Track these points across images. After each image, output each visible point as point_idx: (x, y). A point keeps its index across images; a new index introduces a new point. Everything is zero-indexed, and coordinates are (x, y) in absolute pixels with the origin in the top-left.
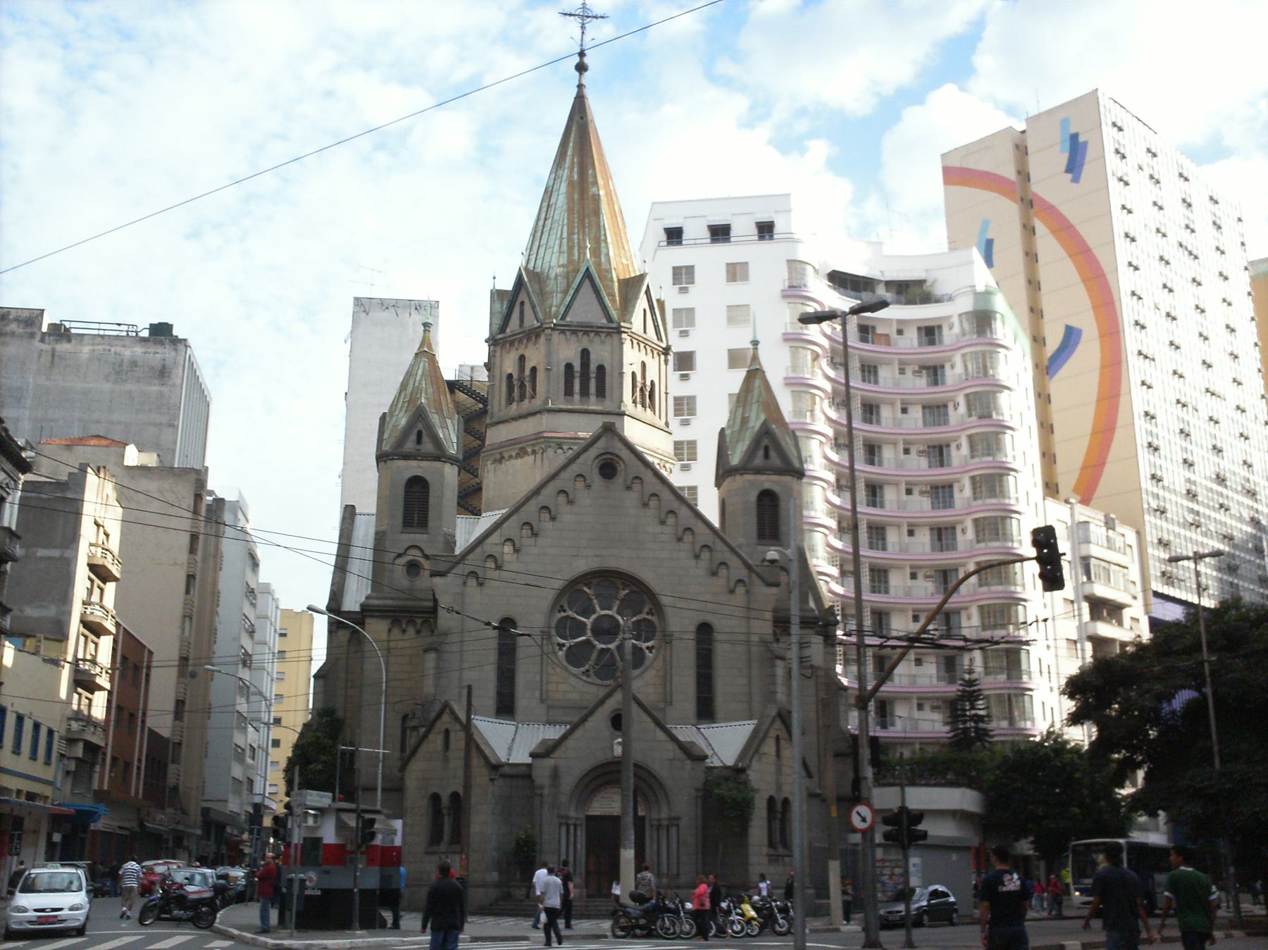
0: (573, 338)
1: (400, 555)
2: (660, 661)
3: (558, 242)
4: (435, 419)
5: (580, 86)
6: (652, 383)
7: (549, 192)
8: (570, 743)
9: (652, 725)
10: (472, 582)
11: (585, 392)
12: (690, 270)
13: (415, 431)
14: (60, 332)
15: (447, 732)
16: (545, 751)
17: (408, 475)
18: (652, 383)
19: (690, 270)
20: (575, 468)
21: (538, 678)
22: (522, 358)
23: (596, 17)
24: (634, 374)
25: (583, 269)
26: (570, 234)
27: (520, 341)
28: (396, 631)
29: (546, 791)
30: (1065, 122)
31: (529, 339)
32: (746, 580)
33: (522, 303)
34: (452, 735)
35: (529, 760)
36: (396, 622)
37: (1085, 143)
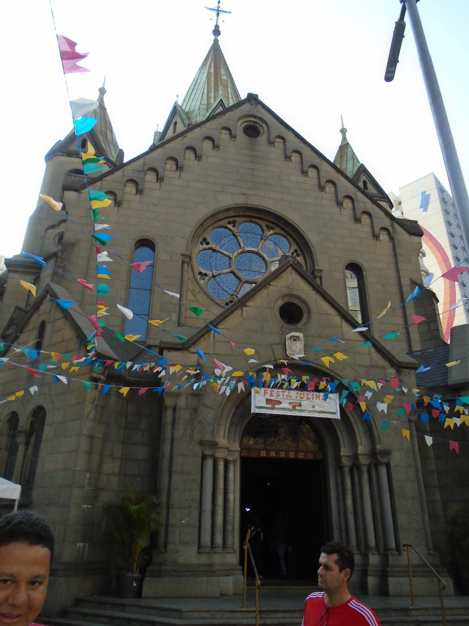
1: (53, 227)
3: (201, 95)
7: (196, 81)
9: (337, 319)
15: (43, 325)
23: (225, 12)
25: (219, 100)
32: (390, 229)
33: (176, 123)
34: (48, 328)
37: (429, 195)
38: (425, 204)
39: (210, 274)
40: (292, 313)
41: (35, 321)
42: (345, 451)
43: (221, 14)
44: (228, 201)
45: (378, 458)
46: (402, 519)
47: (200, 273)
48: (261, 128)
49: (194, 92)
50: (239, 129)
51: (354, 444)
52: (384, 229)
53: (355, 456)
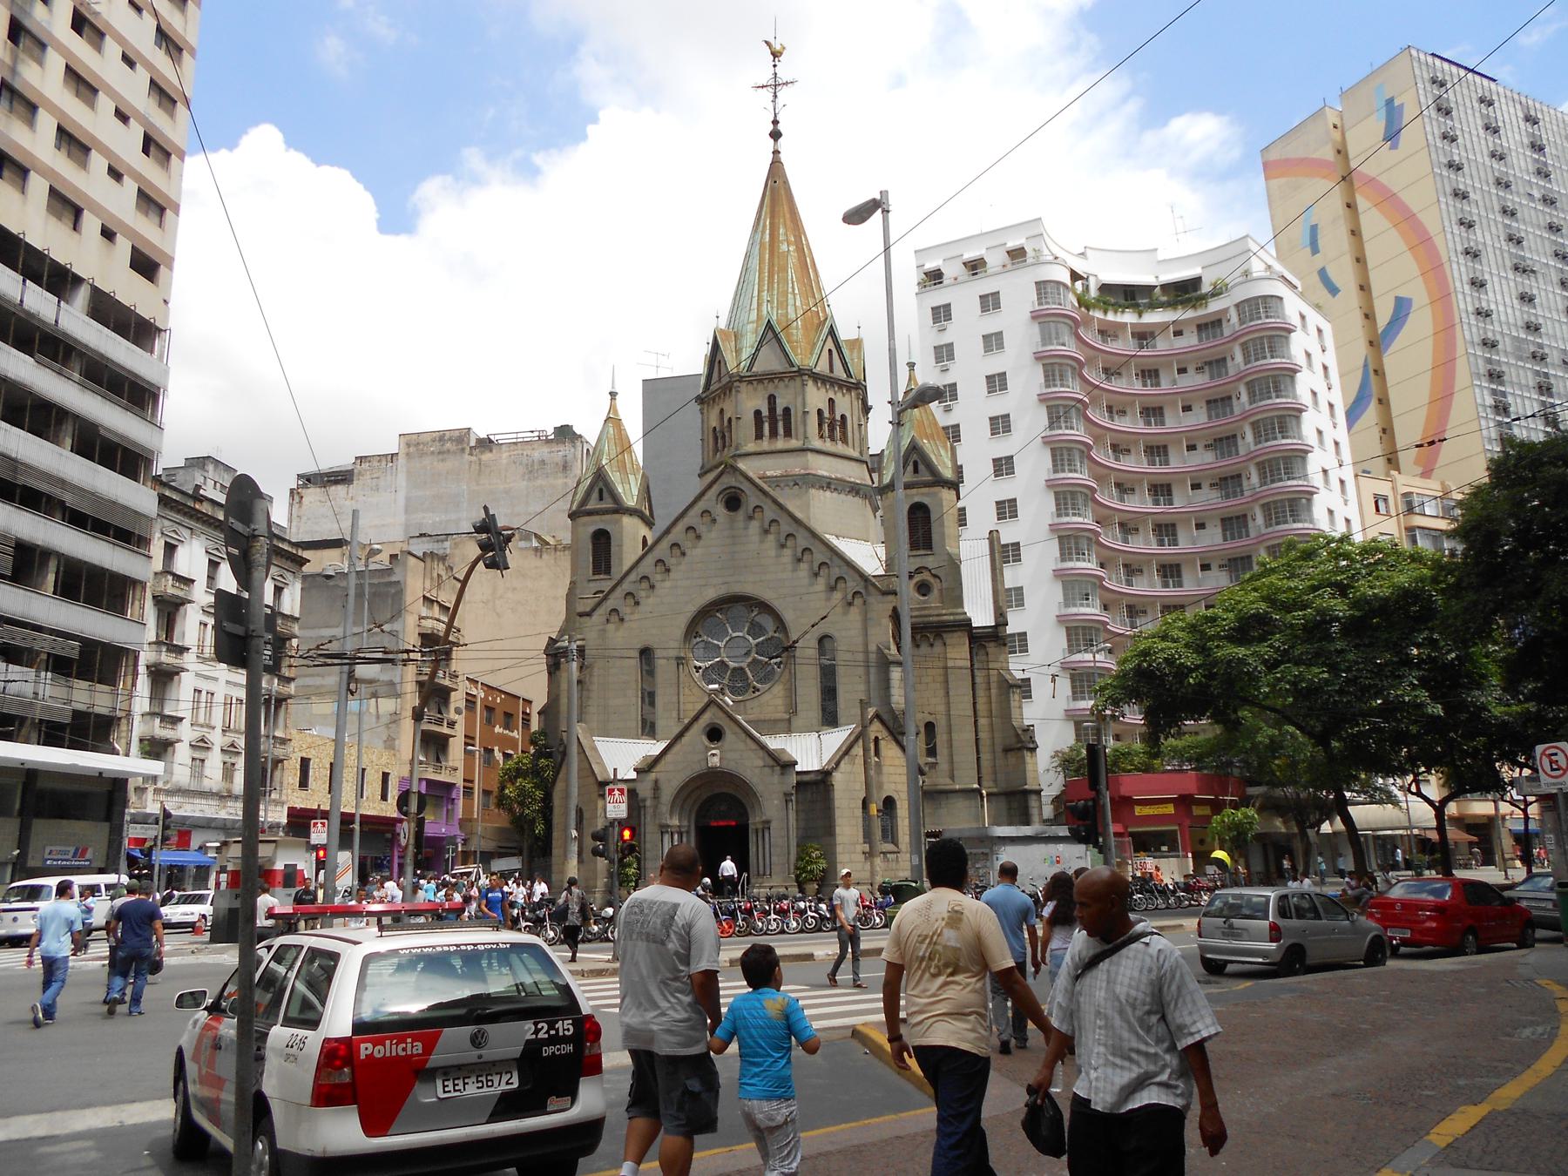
0: (760, 387)
2: (786, 673)
4: (614, 477)
5: (776, 152)
6: (843, 417)
7: (748, 256)
8: (669, 757)
11: (774, 434)
12: (947, 307)
14: (486, 444)
16: (647, 767)
17: (592, 529)
18: (843, 417)
19: (947, 307)
20: (701, 506)
21: (675, 699)
22: (722, 411)
24: (820, 412)
29: (648, 803)
35: (633, 775)
40: (715, 734)
44: (711, 594)
50: (720, 511)
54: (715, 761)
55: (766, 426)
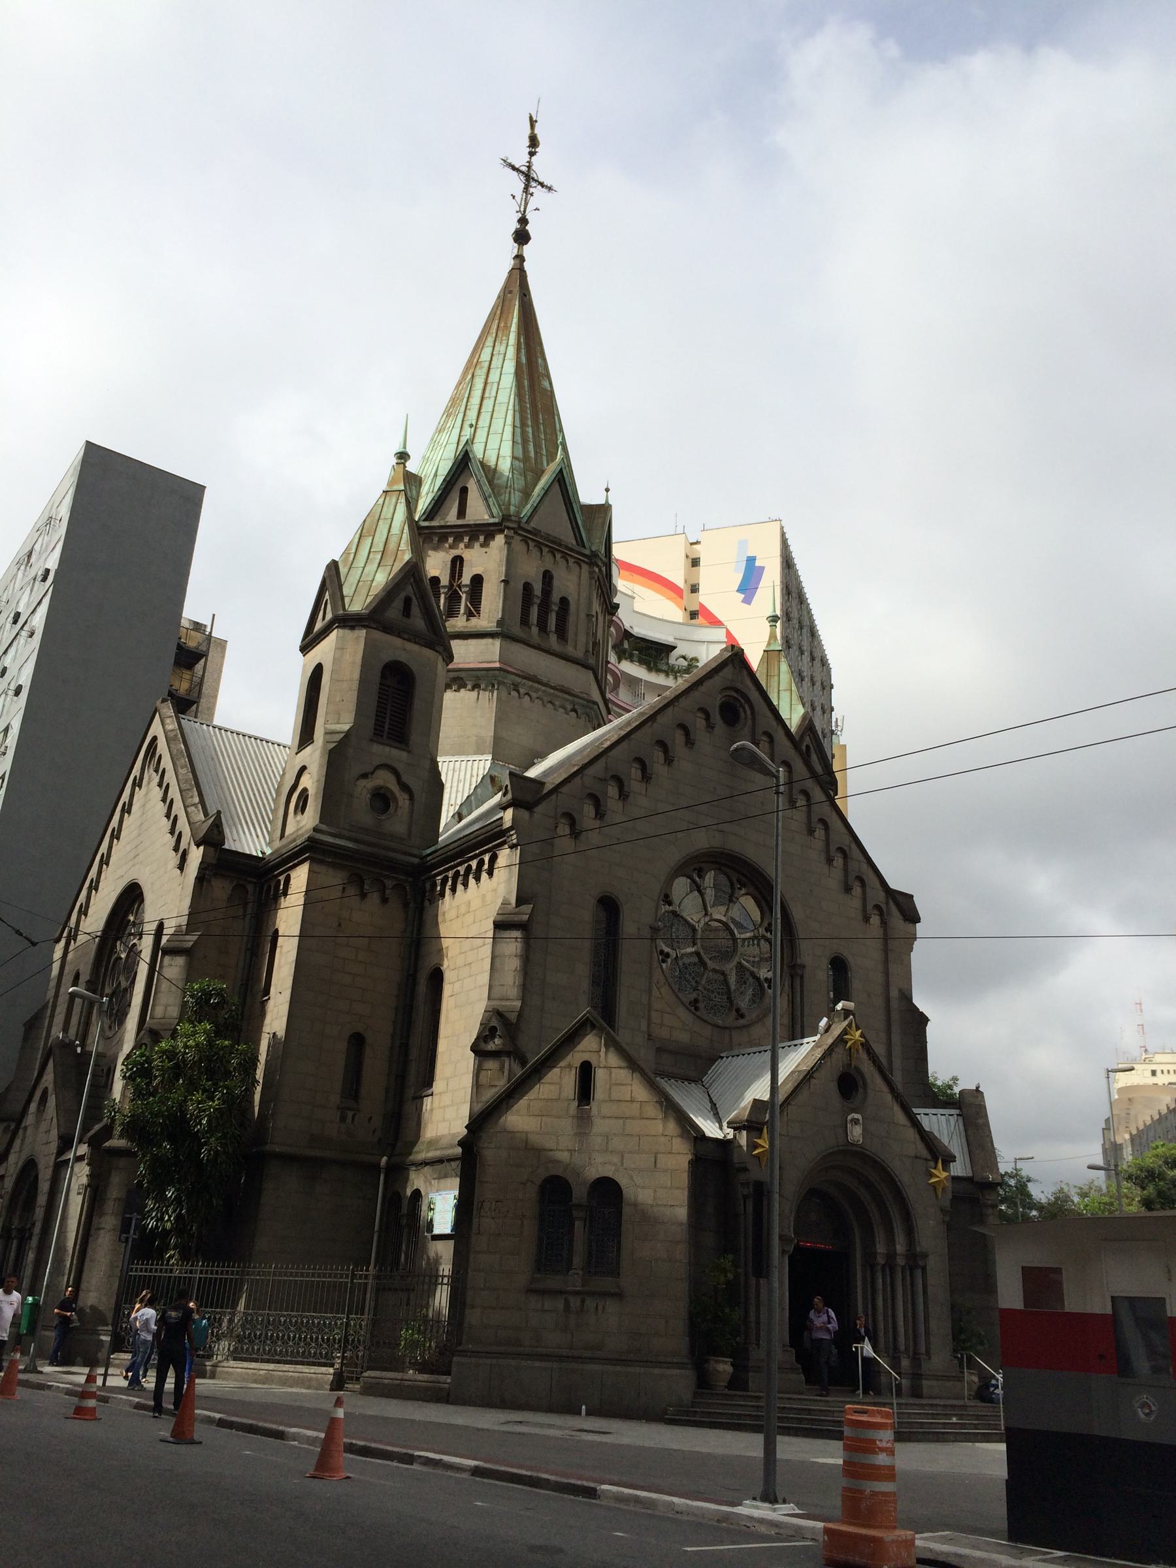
0: (535, 552)
1: (365, 776)
5: (520, 258)
10: (564, 829)
11: (543, 626)
13: (403, 595)
17: (387, 656)
22: (457, 563)
26: (523, 425)
27: (458, 538)
28: (352, 891)
30: (743, 544)
31: (474, 538)
32: (884, 907)
33: (464, 491)
34: (600, 1076)
36: (356, 879)
37: (762, 568)
38: (748, 586)
39: (673, 954)
41: (576, 1058)
42: (881, 1249)
43: (536, 190)
45: (915, 1261)
46: (933, 1324)
47: (662, 952)
48: (741, 710)
49: (488, 405)
51: (891, 1241)
52: (877, 907)
53: (891, 1256)
54: (856, 1133)
55: (534, 612)
